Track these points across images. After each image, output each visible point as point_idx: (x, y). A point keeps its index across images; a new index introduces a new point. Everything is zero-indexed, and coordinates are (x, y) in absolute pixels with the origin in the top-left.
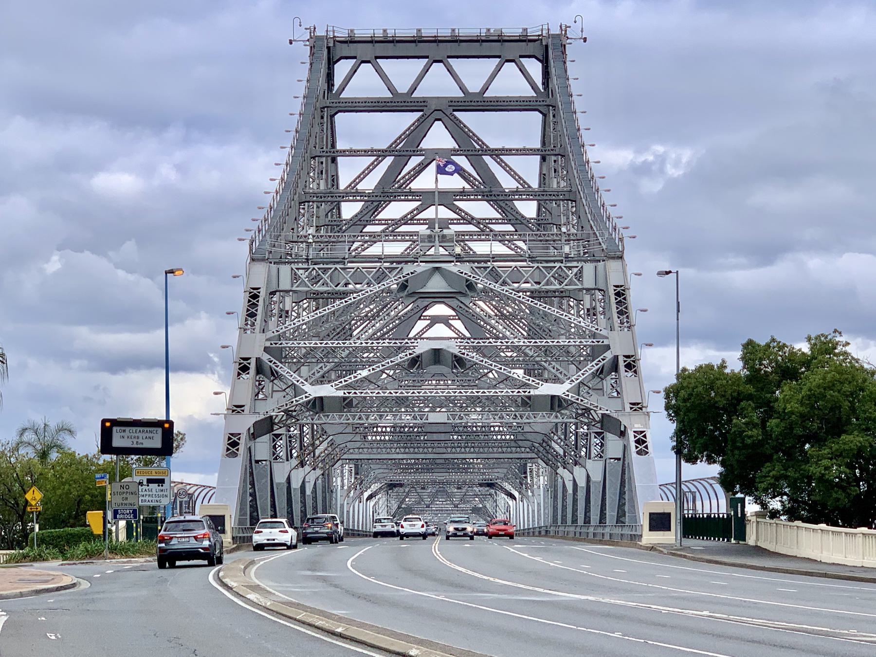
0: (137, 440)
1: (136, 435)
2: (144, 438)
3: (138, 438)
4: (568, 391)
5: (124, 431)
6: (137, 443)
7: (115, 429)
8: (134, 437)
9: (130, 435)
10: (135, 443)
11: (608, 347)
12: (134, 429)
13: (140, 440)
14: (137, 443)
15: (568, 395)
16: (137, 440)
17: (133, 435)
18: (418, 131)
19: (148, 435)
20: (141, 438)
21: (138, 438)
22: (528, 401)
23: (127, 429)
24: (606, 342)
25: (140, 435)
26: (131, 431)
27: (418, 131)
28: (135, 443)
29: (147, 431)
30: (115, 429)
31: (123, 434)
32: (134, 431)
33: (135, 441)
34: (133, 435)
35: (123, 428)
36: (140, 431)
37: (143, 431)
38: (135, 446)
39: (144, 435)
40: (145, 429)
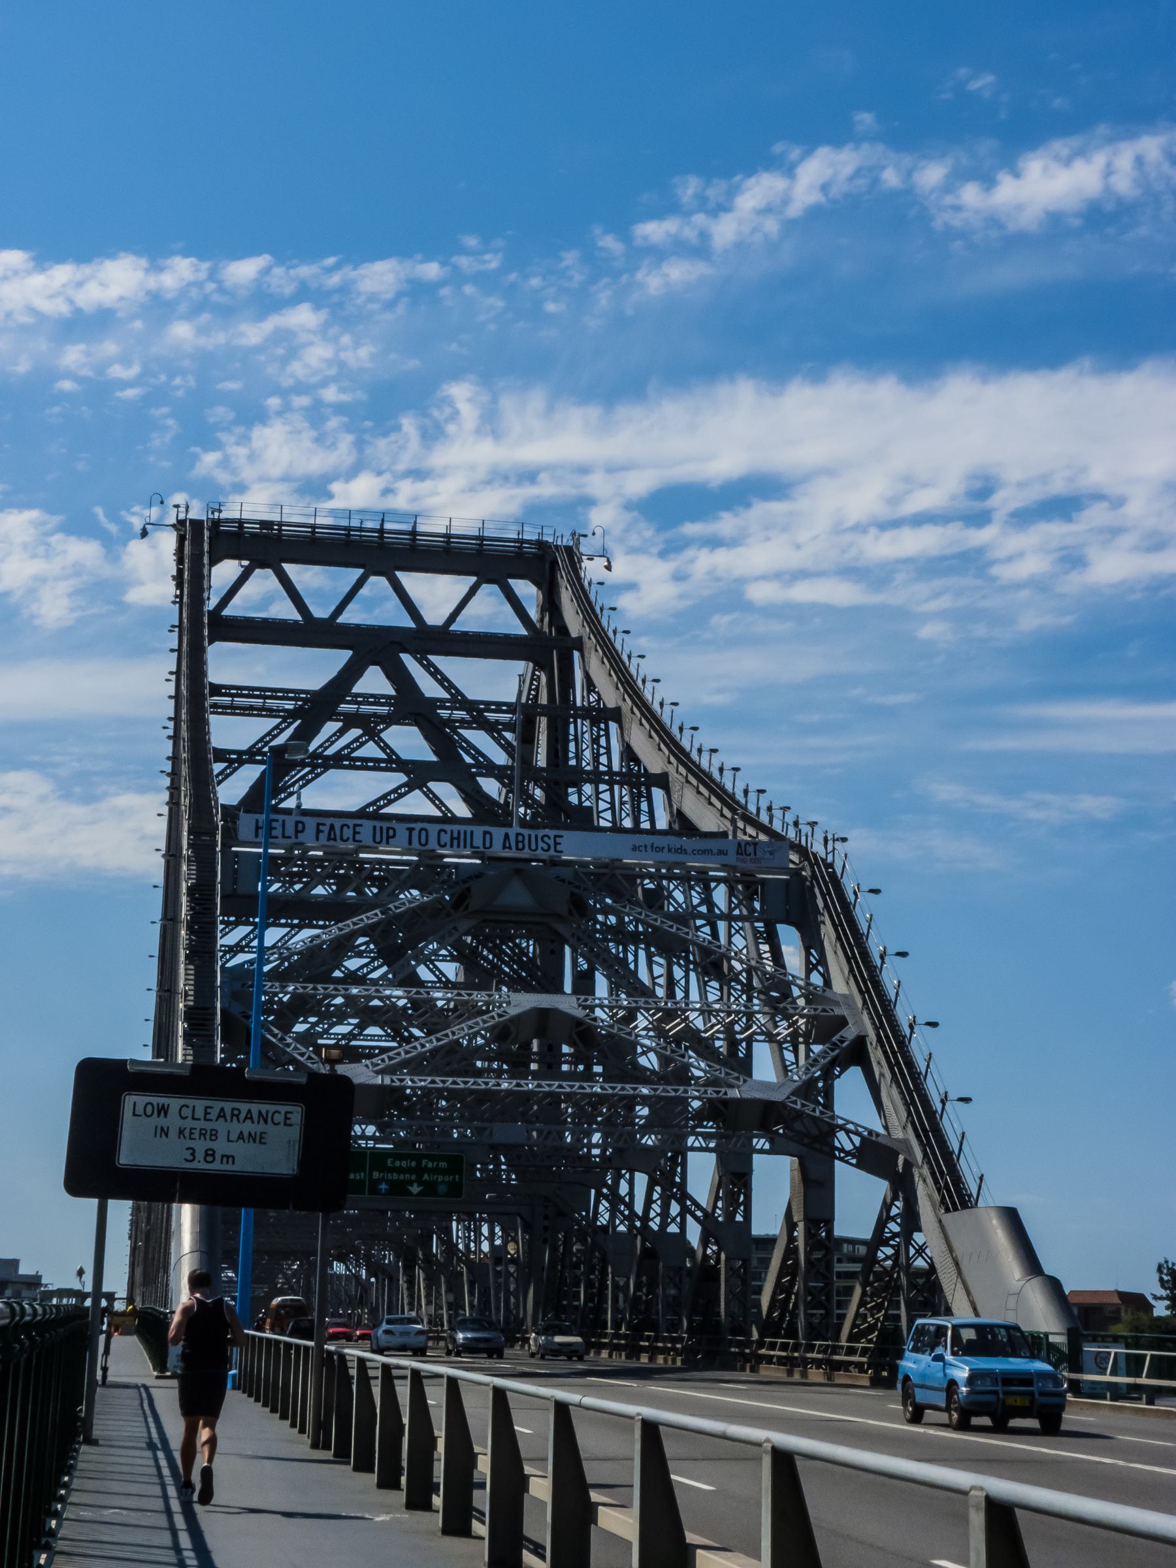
0: (212, 1145)
1: (208, 1126)
2: (234, 1137)
3: (214, 1135)
4: (793, 1093)
5: (163, 1110)
6: (210, 1154)
7: (132, 1102)
8: (203, 1133)
9: (189, 1123)
10: (200, 1155)
11: (842, 1022)
12: (200, 1104)
14: (210, 1154)
15: (795, 1102)
16: (212, 1145)
17: (202, 1124)
18: (351, 673)
19: (247, 1127)
20: (222, 1136)
24: (837, 1012)
25: (221, 1126)
26: (187, 1112)
27: (351, 673)
28: (200, 1155)
30: (132, 1102)
31: (162, 1121)
32: (200, 1113)
33: (201, 1146)
35: (157, 1100)
36: (222, 1114)
37: (235, 1114)
38: (199, 1165)
39: (236, 1127)
40: (244, 1107)
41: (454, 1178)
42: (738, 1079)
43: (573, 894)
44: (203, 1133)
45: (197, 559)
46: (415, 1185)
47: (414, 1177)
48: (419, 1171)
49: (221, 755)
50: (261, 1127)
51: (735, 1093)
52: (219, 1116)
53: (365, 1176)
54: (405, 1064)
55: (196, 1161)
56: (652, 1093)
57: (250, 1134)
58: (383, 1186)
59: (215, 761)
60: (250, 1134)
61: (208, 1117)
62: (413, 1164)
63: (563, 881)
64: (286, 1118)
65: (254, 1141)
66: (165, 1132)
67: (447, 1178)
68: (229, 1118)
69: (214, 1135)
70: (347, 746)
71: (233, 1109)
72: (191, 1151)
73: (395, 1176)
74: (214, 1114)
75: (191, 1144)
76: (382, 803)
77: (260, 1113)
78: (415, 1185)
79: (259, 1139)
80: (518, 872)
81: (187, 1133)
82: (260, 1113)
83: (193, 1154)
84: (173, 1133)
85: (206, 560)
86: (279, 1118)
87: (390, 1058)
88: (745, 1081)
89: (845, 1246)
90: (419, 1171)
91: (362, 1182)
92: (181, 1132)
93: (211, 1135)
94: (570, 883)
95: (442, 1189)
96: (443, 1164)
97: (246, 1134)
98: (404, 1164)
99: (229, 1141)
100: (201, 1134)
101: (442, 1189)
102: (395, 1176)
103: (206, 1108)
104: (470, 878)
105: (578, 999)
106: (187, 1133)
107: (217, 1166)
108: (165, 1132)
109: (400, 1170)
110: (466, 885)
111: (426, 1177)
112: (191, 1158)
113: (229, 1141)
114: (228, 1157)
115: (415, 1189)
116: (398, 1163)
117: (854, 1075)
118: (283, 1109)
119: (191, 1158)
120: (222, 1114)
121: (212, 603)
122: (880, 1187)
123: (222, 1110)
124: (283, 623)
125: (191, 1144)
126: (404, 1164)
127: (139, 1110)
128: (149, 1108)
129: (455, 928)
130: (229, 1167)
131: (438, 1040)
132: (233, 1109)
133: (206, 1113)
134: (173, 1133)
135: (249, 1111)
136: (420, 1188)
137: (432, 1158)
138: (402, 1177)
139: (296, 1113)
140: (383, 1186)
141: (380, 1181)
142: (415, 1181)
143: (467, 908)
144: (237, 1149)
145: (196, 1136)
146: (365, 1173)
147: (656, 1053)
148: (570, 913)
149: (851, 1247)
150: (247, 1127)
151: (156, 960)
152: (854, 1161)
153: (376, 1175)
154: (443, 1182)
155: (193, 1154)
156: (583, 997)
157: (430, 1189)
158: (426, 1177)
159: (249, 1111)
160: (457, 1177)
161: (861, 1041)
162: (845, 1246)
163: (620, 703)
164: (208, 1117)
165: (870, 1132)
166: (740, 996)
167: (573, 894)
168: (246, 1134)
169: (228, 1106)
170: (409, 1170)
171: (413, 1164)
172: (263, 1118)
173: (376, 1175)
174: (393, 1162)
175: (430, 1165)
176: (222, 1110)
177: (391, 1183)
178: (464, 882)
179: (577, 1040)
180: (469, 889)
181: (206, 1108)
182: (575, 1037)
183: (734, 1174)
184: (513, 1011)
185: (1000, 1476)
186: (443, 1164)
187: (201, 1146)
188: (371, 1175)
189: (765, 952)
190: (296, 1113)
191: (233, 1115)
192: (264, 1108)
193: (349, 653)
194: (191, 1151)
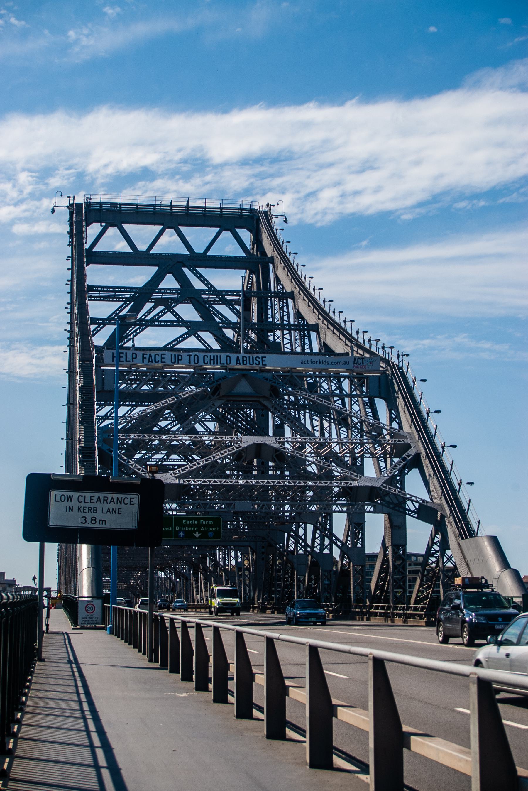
1: (92, 506)
2: (105, 511)
5: (70, 498)
6: (94, 519)
7: (53, 494)
8: (90, 509)
9: (83, 505)
10: (88, 520)
11: (408, 446)
12: (88, 495)
13: (99, 516)
14: (94, 519)
17: (89, 505)
18: (158, 278)
19: (112, 506)
20: (99, 510)
21: (95, 510)
22: (349, 491)
23: (75, 495)
24: (406, 441)
25: (99, 506)
26: (81, 499)
28: (88, 520)
29: (112, 500)
30: (53, 494)
31: (69, 504)
32: (88, 500)
33: (89, 516)
34: (89, 505)
35: (65, 493)
36: (99, 500)
37: (105, 500)
39: (106, 506)
40: (110, 496)
41: (216, 529)
42: (357, 476)
43: (272, 386)
44: (90, 509)
45: (79, 223)
46: (197, 533)
47: (196, 529)
48: (199, 526)
49: (94, 321)
50: (119, 506)
51: (355, 483)
52: (97, 501)
53: (172, 529)
54: (190, 473)
55: (87, 523)
56: (314, 484)
57: (113, 509)
58: (181, 534)
59: (91, 324)
60: (113, 509)
61: (92, 501)
62: (196, 522)
63: (267, 379)
64: (131, 501)
65: (115, 513)
66: (71, 509)
67: (213, 529)
68: (102, 501)
69: (95, 510)
70: (157, 315)
71: (104, 497)
72: (84, 518)
73: (187, 529)
74: (95, 499)
75: (84, 515)
76: (139, 331)
77: (118, 499)
78: (197, 533)
79: (117, 511)
80: (244, 376)
81: (82, 509)
82: (118, 499)
83: (85, 520)
84: (75, 509)
85: (84, 224)
86: (127, 501)
87: (183, 470)
88: (360, 477)
89: (413, 557)
90: (199, 526)
91: (170, 532)
92: (79, 509)
93: (94, 510)
94: (270, 381)
95: (211, 534)
96: (211, 522)
97: (111, 510)
98: (191, 522)
99: (102, 513)
100: (89, 510)
101: (211, 534)
102: (187, 529)
103: (91, 497)
104: (220, 379)
105: (276, 439)
106: (82, 509)
107: (97, 525)
108: (71, 509)
109: (189, 526)
110: (219, 383)
111: (202, 529)
112: (84, 522)
113: (102, 513)
114: (103, 521)
115: (197, 535)
116: (188, 522)
117: (415, 472)
118: (129, 496)
119: (84, 522)
120: (99, 500)
121: (87, 246)
122: (429, 528)
123: (99, 497)
124: (124, 253)
125: (84, 515)
126: (191, 522)
127: (58, 499)
128: (63, 497)
129: (213, 405)
130: (104, 526)
131: (206, 461)
132: (104, 497)
133: (91, 499)
134: (75, 509)
135: (112, 498)
136: (200, 534)
137: (205, 519)
138: (190, 529)
139: (136, 498)
140: (181, 534)
141: (179, 531)
142: (197, 531)
143: (219, 394)
144: (107, 517)
145: (87, 510)
146: (172, 527)
147: (316, 464)
148: (271, 395)
149: (415, 558)
150: (112, 506)
151: (65, 424)
152: (416, 516)
153: (177, 528)
154: (211, 531)
155: (85, 520)
156: (278, 438)
157: (204, 535)
158: (202, 529)
159: (112, 498)
160: (218, 528)
161: (418, 456)
162: (413, 557)
163: (294, 289)
164: (92, 501)
165: (424, 501)
166: (357, 435)
167: (272, 386)
168: (111, 510)
169: (102, 496)
170: (194, 526)
171: (196, 522)
172: (119, 501)
173: (177, 528)
174: (186, 522)
175: (204, 523)
176: (99, 497)
177: (185, 532)
178: (217, 381)
179: (276, 460)
180: (219, 385)
181: (91, 497)
182: (275, 457)
183: (356, 524)
184: (243, 445)
185: (363, 647)
186: (211, 522)
187: (89, 516)
188: (175, 528)
189: (369, 413)
190: (136, 498)
191: (104, 500)
192: (120, 496)
193: (157, 268)
194: (84, 518)
